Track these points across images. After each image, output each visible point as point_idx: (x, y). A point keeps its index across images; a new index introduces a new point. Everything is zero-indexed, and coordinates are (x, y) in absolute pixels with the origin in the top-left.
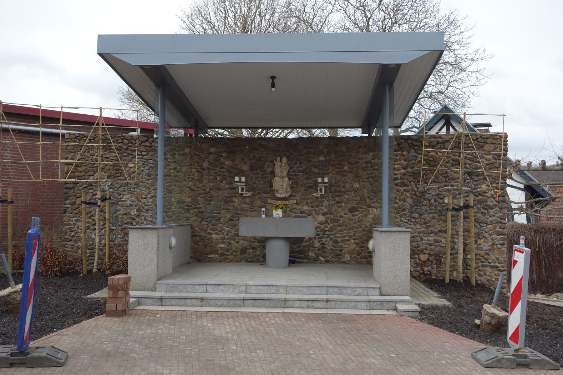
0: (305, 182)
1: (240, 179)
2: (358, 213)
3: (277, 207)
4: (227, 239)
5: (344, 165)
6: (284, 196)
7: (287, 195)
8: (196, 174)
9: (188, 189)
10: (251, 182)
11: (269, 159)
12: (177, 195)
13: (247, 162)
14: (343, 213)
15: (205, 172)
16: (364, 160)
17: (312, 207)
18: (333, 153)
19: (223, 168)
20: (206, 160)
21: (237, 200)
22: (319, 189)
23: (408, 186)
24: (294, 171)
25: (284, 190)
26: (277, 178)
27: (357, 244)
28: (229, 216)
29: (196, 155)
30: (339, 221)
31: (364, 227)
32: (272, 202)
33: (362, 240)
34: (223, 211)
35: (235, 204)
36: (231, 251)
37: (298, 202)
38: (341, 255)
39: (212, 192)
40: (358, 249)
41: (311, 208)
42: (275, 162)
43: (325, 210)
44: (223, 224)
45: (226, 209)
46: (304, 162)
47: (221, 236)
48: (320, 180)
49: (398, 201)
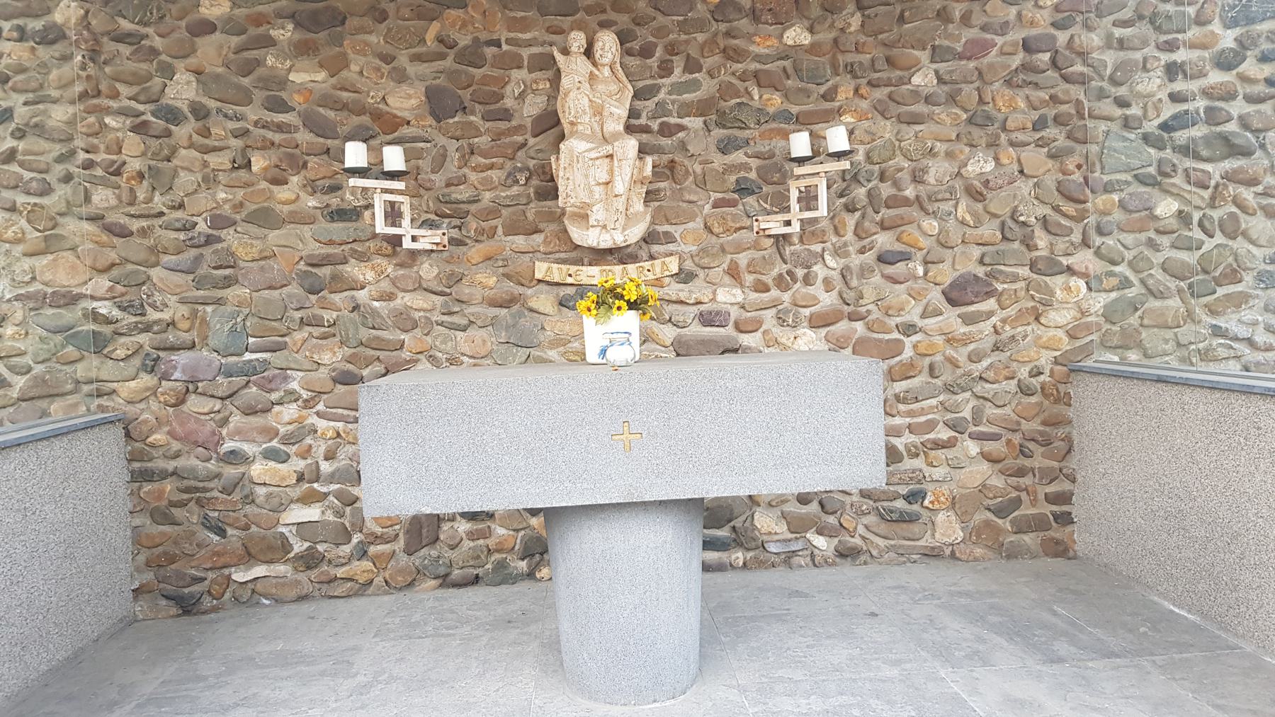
0: (719, 161)
1: (376, 152)
2: (991, 304)
3: (608, 298)
4: (332, 478)
5: (914, 67)
6: (619, 239)
7: (635, 233)
8: (133, 144)
9: (87, 226)
10: (438, 179)
11: (525, 53)
12: (27, 263)
13: (412, 69)
14: (919, 310)
15: (182, 132)
16: (1016, 35)
17: (762, 288)
18: (851, 7)
19: (282, 107)
20: (180, 65)
21: (370, 276)
22: (794, 195)
23: (1247, 153)
24: (661, 110)
25: (620, 204)
26: (573, 146)
27: (986, 456)
28: (332, 356)
29: (121, 38)
30: (896, 348)
31: (1023, 372)
32: (557, 272)
33: (1017, 439)
34: (299, 336)
35: (362, 295)
36: (356, 538)
37: (689, 265)
38: (910, 519)
39: (230, 237)
40: (998, 482)
41: (754, 296)
42: (559, 57)
43: (827, 300)
44: (308, 404)
45: (316, 322)
46: (708, 63)
47: (300, 464)
48: (800, 144)
49: (1197, 234)
